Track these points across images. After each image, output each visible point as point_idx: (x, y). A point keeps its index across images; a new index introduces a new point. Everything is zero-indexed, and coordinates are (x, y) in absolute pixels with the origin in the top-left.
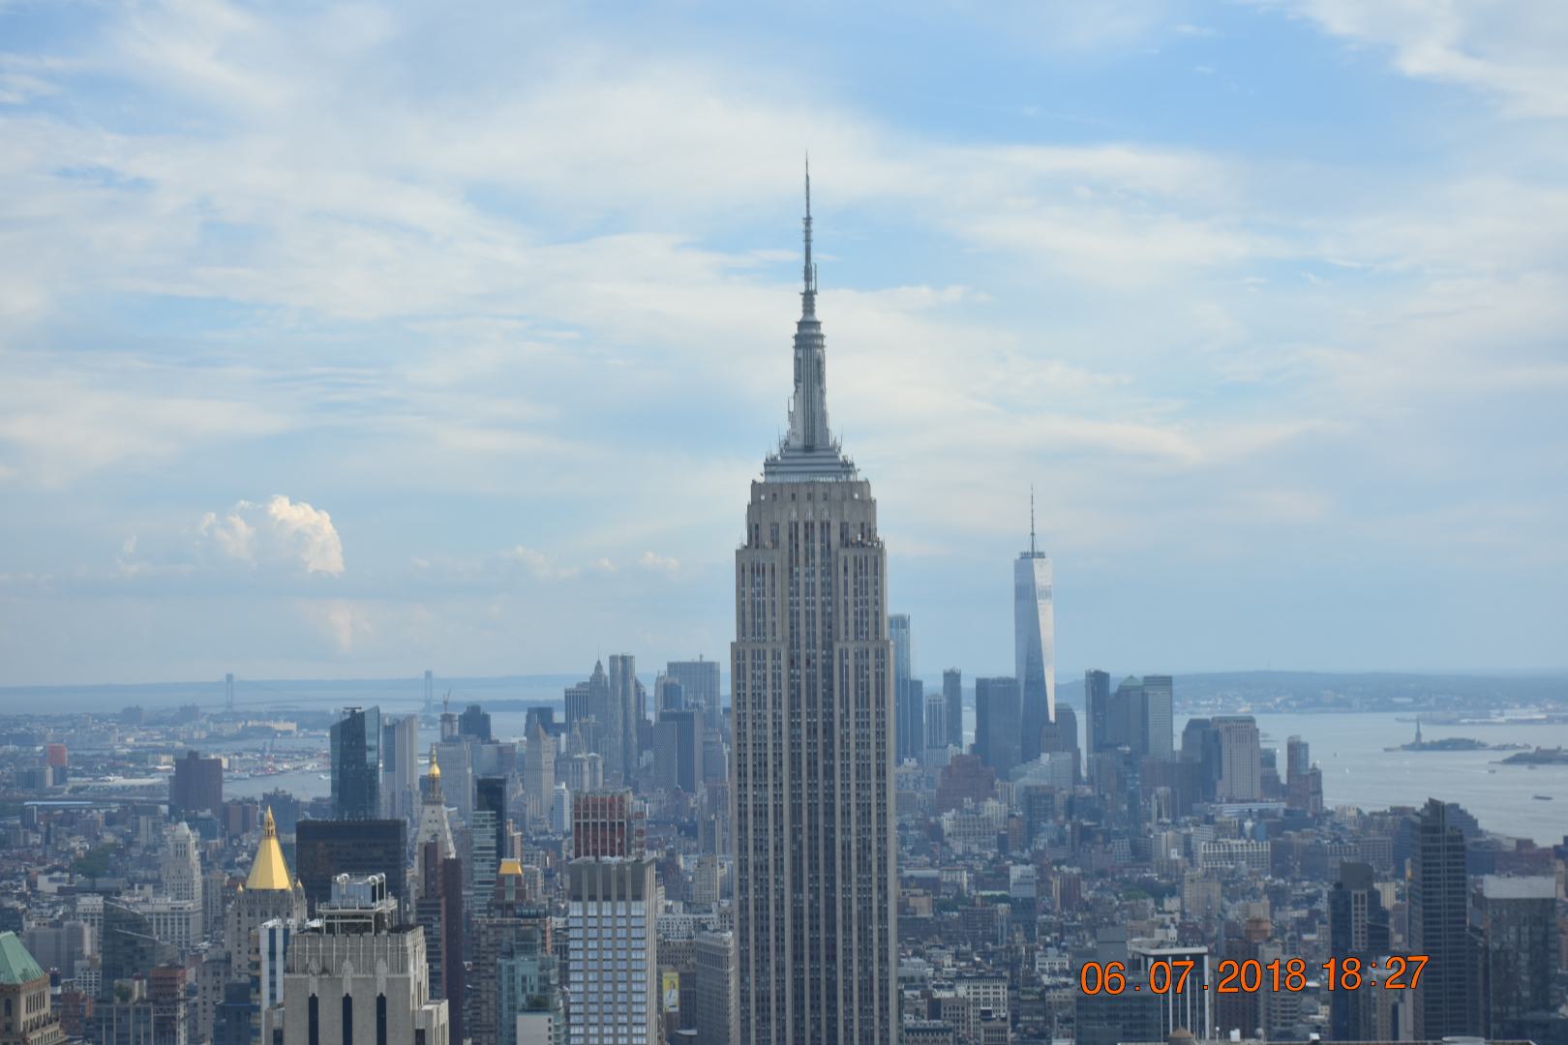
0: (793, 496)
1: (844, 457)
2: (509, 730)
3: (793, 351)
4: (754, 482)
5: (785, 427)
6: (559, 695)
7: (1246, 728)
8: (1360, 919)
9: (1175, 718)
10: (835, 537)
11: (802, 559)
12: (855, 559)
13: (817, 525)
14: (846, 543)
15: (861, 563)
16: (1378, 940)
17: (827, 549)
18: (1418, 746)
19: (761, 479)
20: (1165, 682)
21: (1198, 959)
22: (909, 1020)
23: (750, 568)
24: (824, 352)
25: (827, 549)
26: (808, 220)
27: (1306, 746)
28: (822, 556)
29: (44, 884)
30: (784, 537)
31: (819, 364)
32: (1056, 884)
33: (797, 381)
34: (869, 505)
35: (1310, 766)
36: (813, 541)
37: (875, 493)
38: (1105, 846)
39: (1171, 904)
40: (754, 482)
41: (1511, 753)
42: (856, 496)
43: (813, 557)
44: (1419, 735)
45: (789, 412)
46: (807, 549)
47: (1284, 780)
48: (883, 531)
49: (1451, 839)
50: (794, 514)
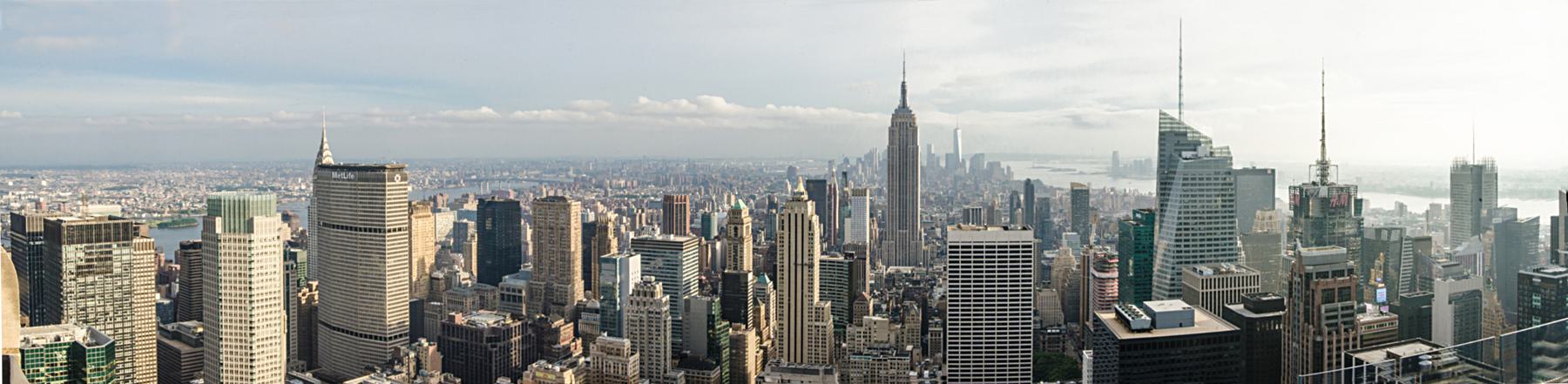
2: (853, 162)
5: (897, 103)
7: (999, 164)
8: (1015, 202)
14: (910, 126)
16: (1019, 205)
17: (907, 128)
18: (1034, 168)
20: (983, 155)
21: (980, 209)
22: (925, 220)
23: (891, 132)
25: (907, 128)
29: (762, 191)
32: (959, 195)
34: (914, 119)
37: (916, 116)
39: (981, 198)
48: (918, 122)
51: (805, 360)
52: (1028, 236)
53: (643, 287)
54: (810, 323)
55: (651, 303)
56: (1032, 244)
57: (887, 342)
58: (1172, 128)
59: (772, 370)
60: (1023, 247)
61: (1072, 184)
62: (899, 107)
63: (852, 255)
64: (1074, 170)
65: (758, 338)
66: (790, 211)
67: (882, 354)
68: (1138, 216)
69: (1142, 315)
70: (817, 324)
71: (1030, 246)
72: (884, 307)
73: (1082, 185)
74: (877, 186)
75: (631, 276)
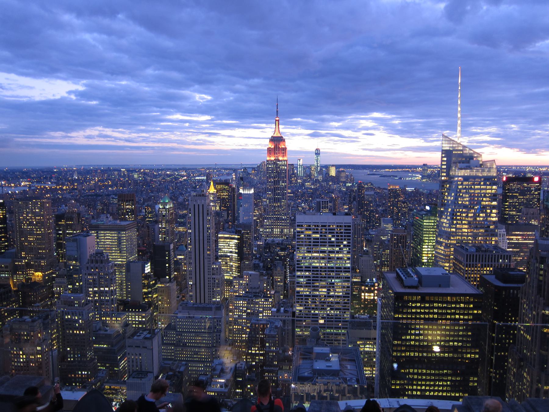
6: (256, 166)
51: (207, 301)
52: (349, 219)
53: (95, 257)
54: (209, 276)
55: (101, 268)
56: (351, 225)
57: (258, 288)
58: (450, 147)
59: (183, 309)
60: (345, 226)
63: (240, 231)
65: (178, 287)
66: (194, 203)
67: (254, 296)
68: (428, 208)
69: (413, 276)
70: (214, 276)
71: (350, 226)
72: (261, 265)
74: (264, 186)
75: (88, 250)
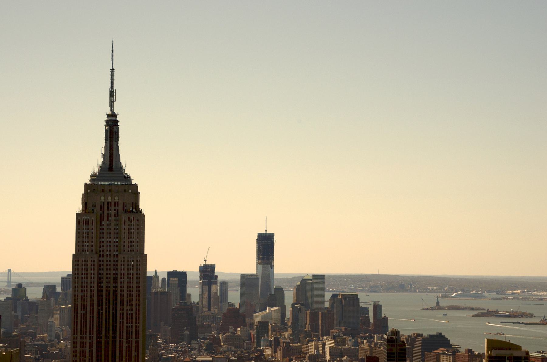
0: (103, 190)
1: (126, 174)
3: (105, 127)
4: (86, 185)
6: (60, 281)
7: (355, 299)
9: (326, 293)
10: (120, 208)
11: (106, 218)
12: (129, 218)
13: (113, 204)
15: (131, 220)
17: (117, 215)
18: (438, 307)
19: (88, 182)
23: (81, 220)
24: (118, 129)
25: (117, 215)
26: (112, 70)
27: (381, 306)
28: (115, 216)
30: (98, 207)
31: (117, 133)
33: (106, 140)
35: (383, 316)
36: (111, 210)
37: (139, 191)
38: (288, 349)
40: (86, 185)
41: (475, 312)
42: (130, 191)
43: (110, 216)
44: (438, 303)
45: (102, 154)
46: (108, 214)
47: (372, 321)
48: (143, 206)
49: (400, 346)
50: (102, 199)
61: (493, 344)
62: (102, 168)
64: (531, 316)
73: (518, 348)
